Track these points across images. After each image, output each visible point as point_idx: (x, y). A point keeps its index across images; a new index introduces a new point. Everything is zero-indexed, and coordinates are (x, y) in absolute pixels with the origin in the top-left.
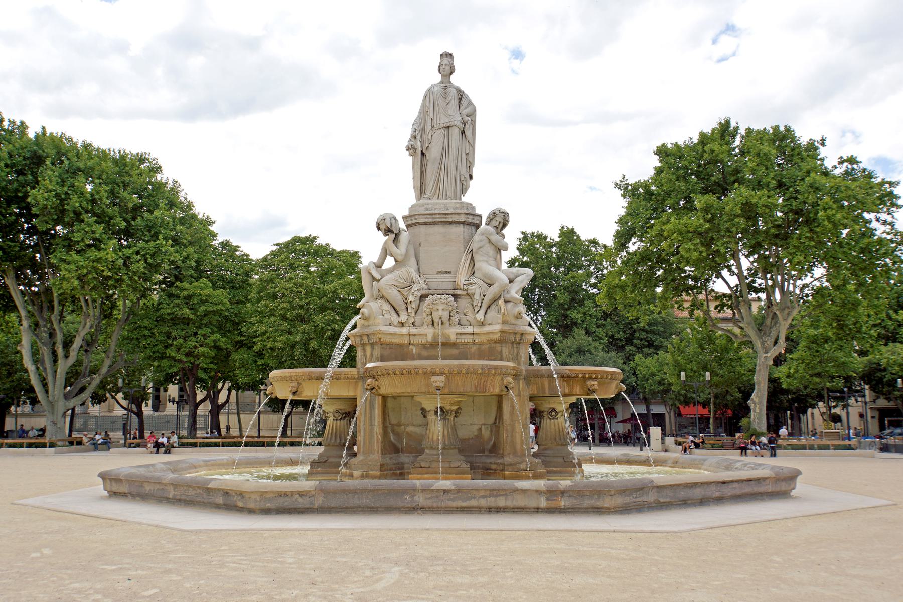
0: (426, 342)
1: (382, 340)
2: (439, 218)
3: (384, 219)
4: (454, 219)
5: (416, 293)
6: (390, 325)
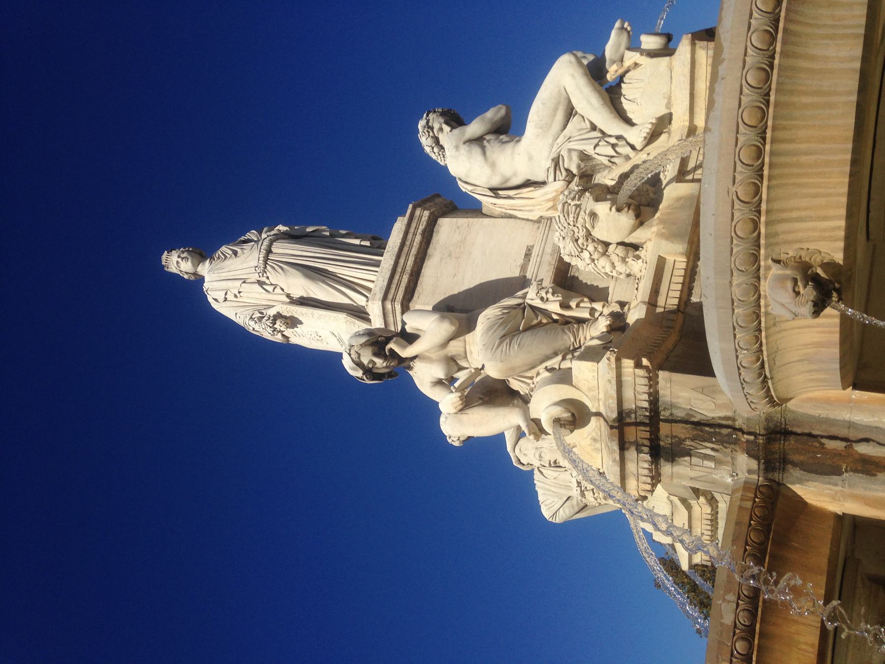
2: (406, 260)
4: (420, 231)
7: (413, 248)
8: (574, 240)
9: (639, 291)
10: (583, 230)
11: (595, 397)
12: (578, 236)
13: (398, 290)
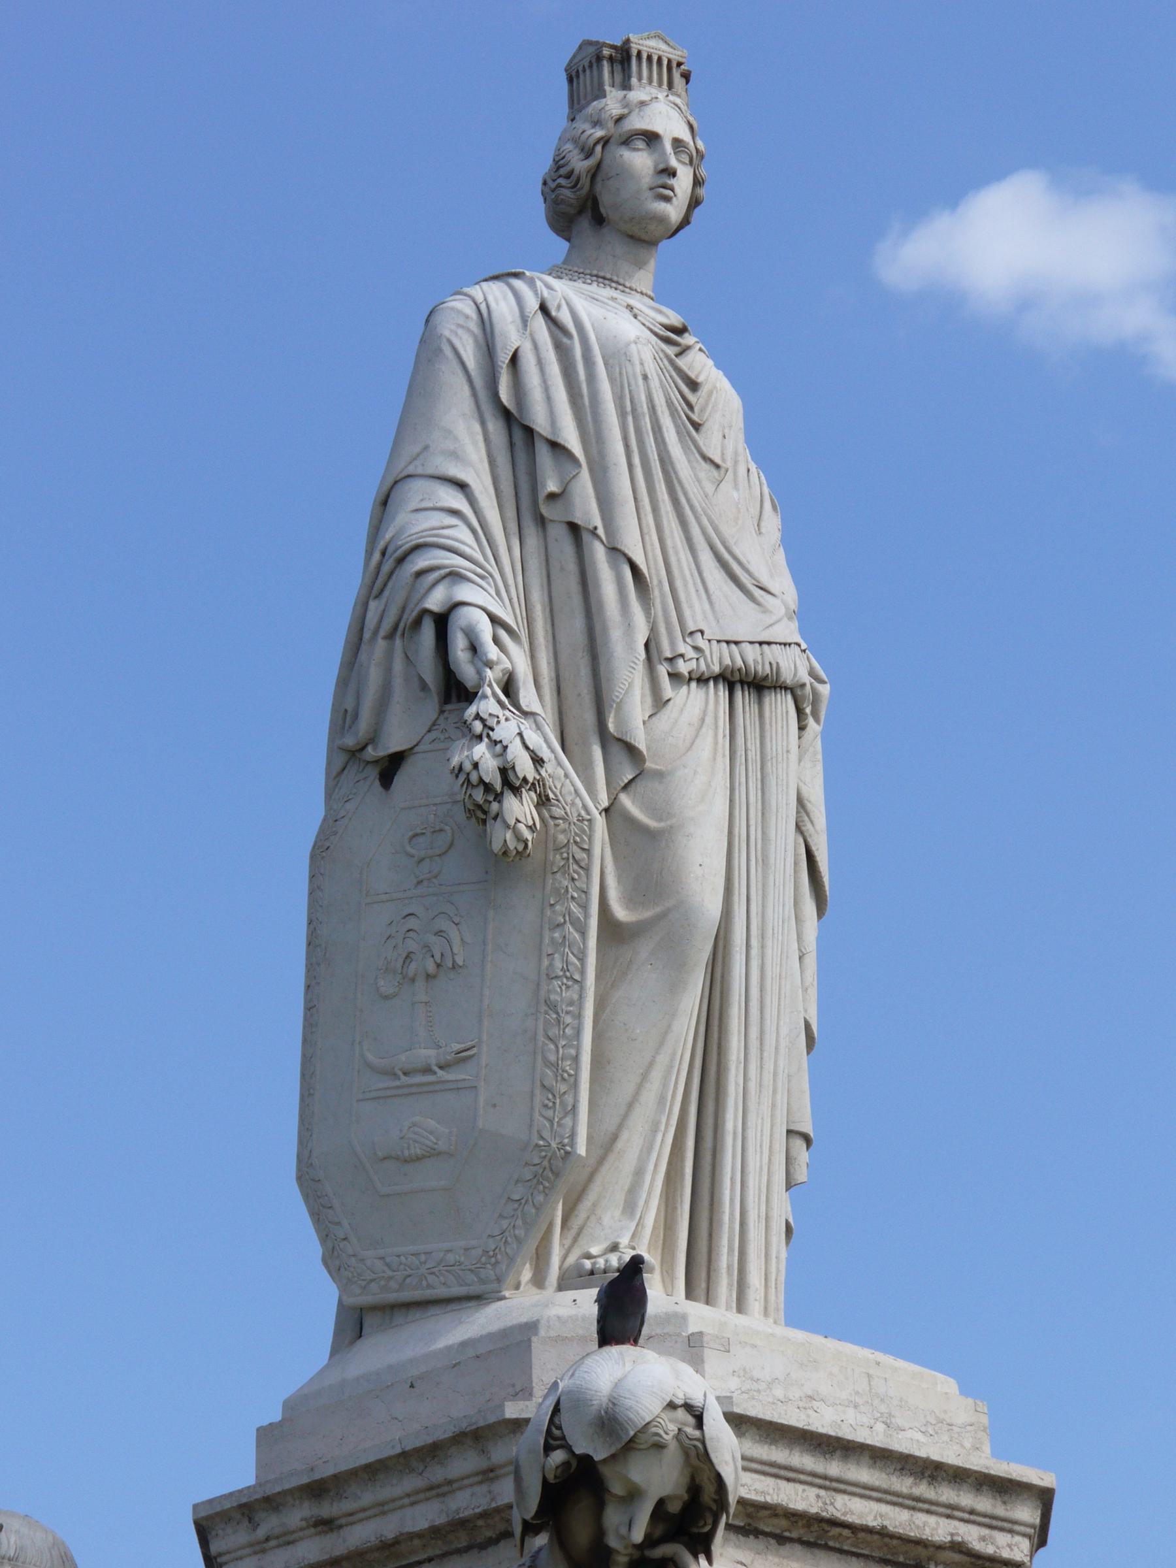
2: (866, 1492)
7: (904, 1515)
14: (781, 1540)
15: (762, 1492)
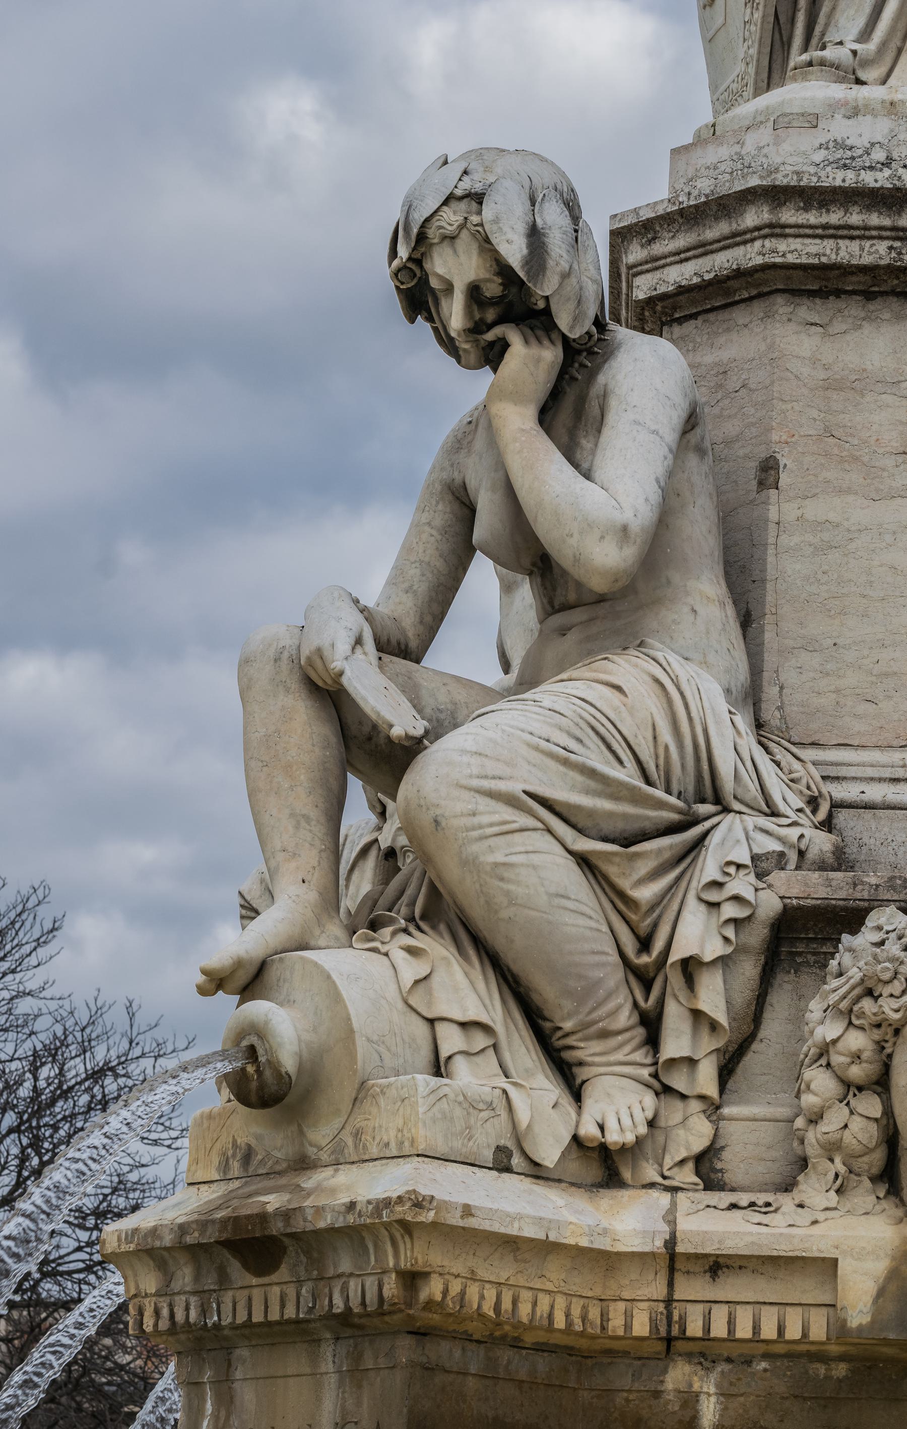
0: (818, 1332)
1: (433, 1289)
3: (478, 198)
5: (742, 885)
6: (502, 1165)
8: (869, 984)
9: (729, 1214)
10: (897, 1011)
11: (342, 1152)
12: (881, 995)
13: (822, 237)
14: (869, 296)
15: (816, 255)
